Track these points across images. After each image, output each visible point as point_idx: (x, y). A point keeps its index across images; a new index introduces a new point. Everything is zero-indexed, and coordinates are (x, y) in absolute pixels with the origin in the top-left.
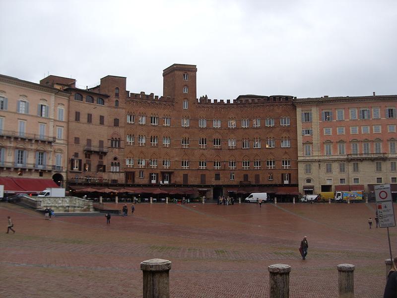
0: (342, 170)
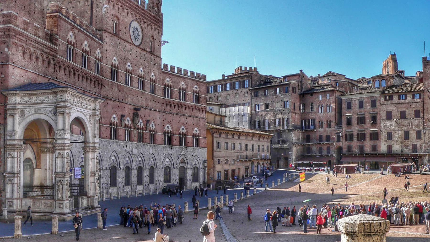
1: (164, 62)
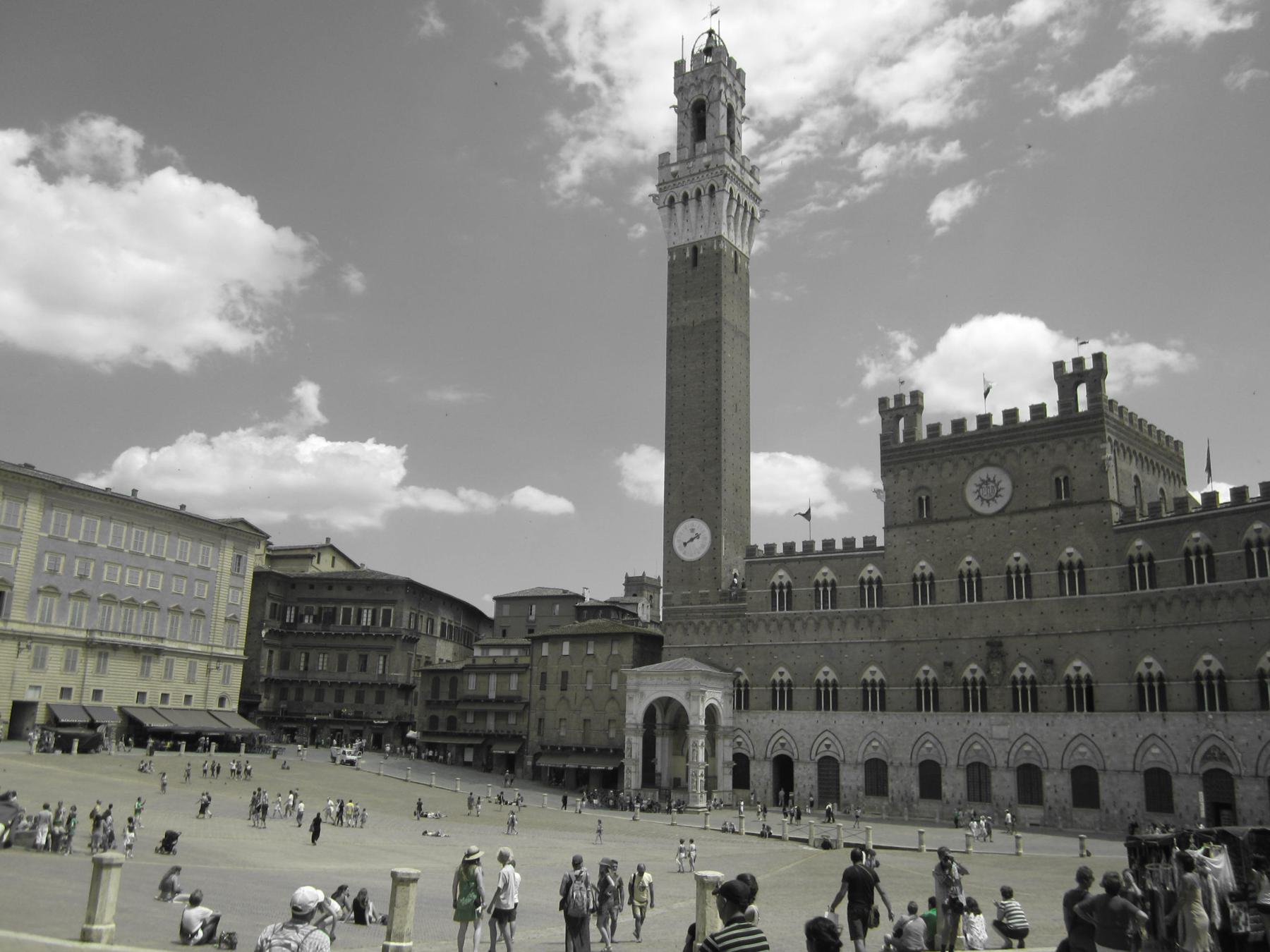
0: (69, 666)
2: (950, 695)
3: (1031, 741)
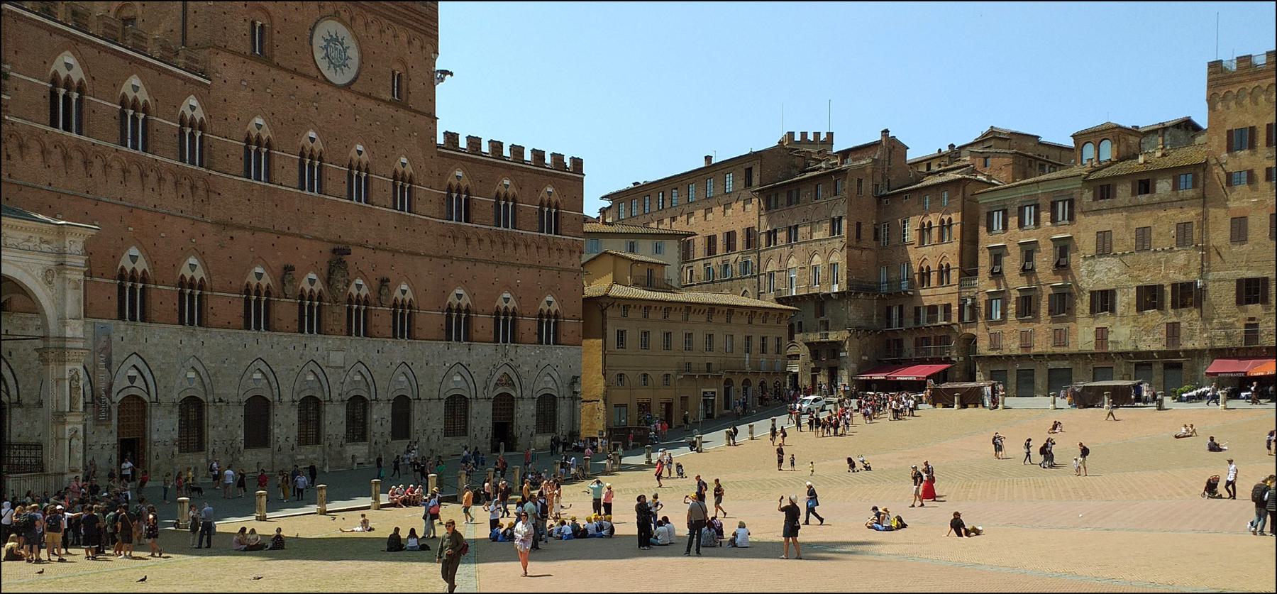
1: (443, 126)
2: (286, 309)
3: (364, 370)
